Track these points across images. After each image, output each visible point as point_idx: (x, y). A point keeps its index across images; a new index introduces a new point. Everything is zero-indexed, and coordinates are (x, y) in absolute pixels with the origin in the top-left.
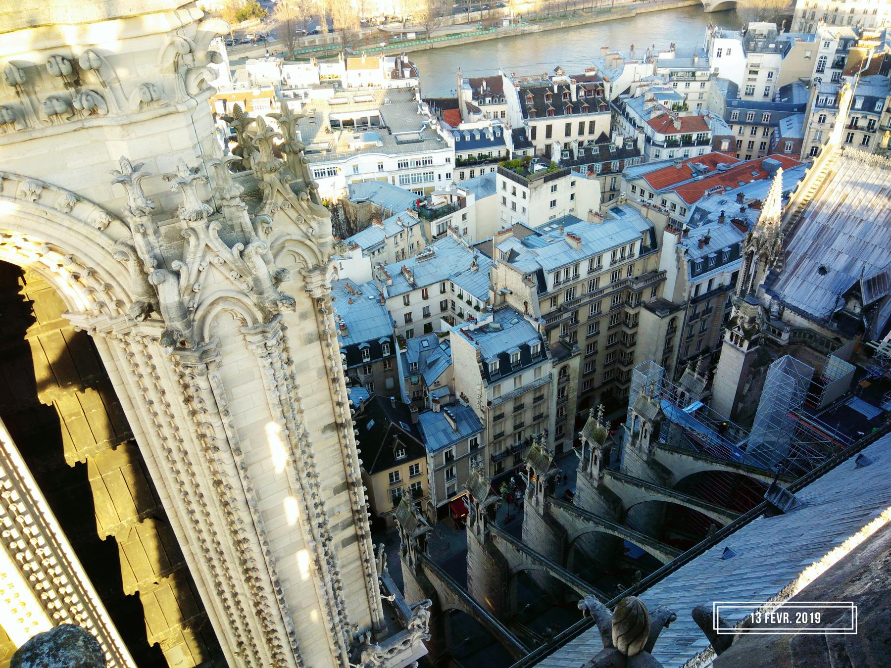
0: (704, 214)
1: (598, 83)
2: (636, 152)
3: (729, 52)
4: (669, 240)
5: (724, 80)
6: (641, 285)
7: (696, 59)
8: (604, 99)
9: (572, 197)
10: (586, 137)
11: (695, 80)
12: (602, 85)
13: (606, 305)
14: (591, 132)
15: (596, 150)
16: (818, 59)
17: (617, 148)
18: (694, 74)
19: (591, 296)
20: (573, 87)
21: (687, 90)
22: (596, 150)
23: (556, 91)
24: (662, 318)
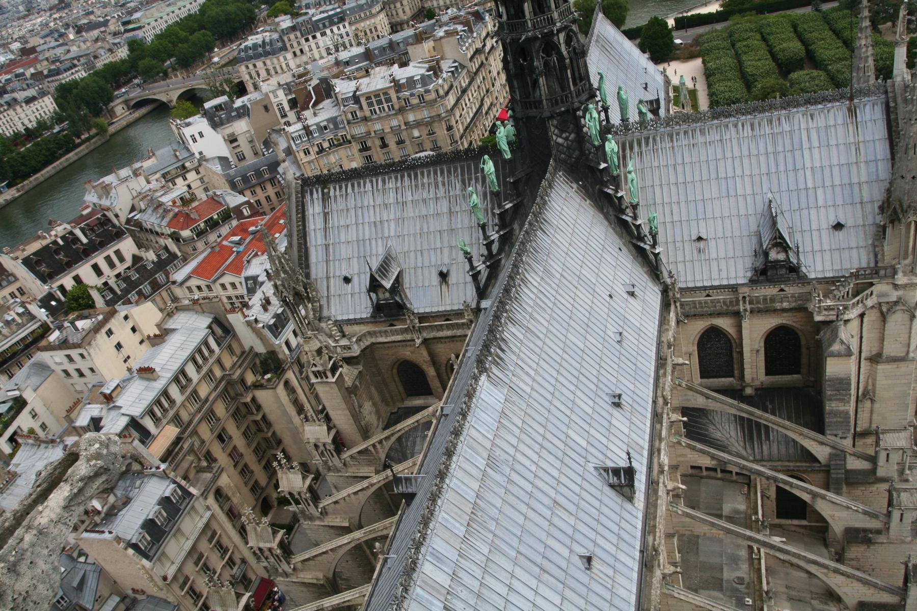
0: (254, 279)
1: (99, 216)
2: (173, 256)
3: (201, 135)
4: (236, 320)
5: (213, 159)
6: (239, 372)
7: (178, 154)
8: (114, 226)
9: (134, 330)
10: (120, 268)
11: (188, 171)
12: (104, 215)
13: (220, 409)
14: (122, 259)
15: (135, 276)
16: (276, 108)
17: (153, 262)
18: (183, 167)
19: (199, 410)
20: (78, 232)
21: (187, 182)
22: (135, 276)
23: (61, 242)
24: (275, 388)
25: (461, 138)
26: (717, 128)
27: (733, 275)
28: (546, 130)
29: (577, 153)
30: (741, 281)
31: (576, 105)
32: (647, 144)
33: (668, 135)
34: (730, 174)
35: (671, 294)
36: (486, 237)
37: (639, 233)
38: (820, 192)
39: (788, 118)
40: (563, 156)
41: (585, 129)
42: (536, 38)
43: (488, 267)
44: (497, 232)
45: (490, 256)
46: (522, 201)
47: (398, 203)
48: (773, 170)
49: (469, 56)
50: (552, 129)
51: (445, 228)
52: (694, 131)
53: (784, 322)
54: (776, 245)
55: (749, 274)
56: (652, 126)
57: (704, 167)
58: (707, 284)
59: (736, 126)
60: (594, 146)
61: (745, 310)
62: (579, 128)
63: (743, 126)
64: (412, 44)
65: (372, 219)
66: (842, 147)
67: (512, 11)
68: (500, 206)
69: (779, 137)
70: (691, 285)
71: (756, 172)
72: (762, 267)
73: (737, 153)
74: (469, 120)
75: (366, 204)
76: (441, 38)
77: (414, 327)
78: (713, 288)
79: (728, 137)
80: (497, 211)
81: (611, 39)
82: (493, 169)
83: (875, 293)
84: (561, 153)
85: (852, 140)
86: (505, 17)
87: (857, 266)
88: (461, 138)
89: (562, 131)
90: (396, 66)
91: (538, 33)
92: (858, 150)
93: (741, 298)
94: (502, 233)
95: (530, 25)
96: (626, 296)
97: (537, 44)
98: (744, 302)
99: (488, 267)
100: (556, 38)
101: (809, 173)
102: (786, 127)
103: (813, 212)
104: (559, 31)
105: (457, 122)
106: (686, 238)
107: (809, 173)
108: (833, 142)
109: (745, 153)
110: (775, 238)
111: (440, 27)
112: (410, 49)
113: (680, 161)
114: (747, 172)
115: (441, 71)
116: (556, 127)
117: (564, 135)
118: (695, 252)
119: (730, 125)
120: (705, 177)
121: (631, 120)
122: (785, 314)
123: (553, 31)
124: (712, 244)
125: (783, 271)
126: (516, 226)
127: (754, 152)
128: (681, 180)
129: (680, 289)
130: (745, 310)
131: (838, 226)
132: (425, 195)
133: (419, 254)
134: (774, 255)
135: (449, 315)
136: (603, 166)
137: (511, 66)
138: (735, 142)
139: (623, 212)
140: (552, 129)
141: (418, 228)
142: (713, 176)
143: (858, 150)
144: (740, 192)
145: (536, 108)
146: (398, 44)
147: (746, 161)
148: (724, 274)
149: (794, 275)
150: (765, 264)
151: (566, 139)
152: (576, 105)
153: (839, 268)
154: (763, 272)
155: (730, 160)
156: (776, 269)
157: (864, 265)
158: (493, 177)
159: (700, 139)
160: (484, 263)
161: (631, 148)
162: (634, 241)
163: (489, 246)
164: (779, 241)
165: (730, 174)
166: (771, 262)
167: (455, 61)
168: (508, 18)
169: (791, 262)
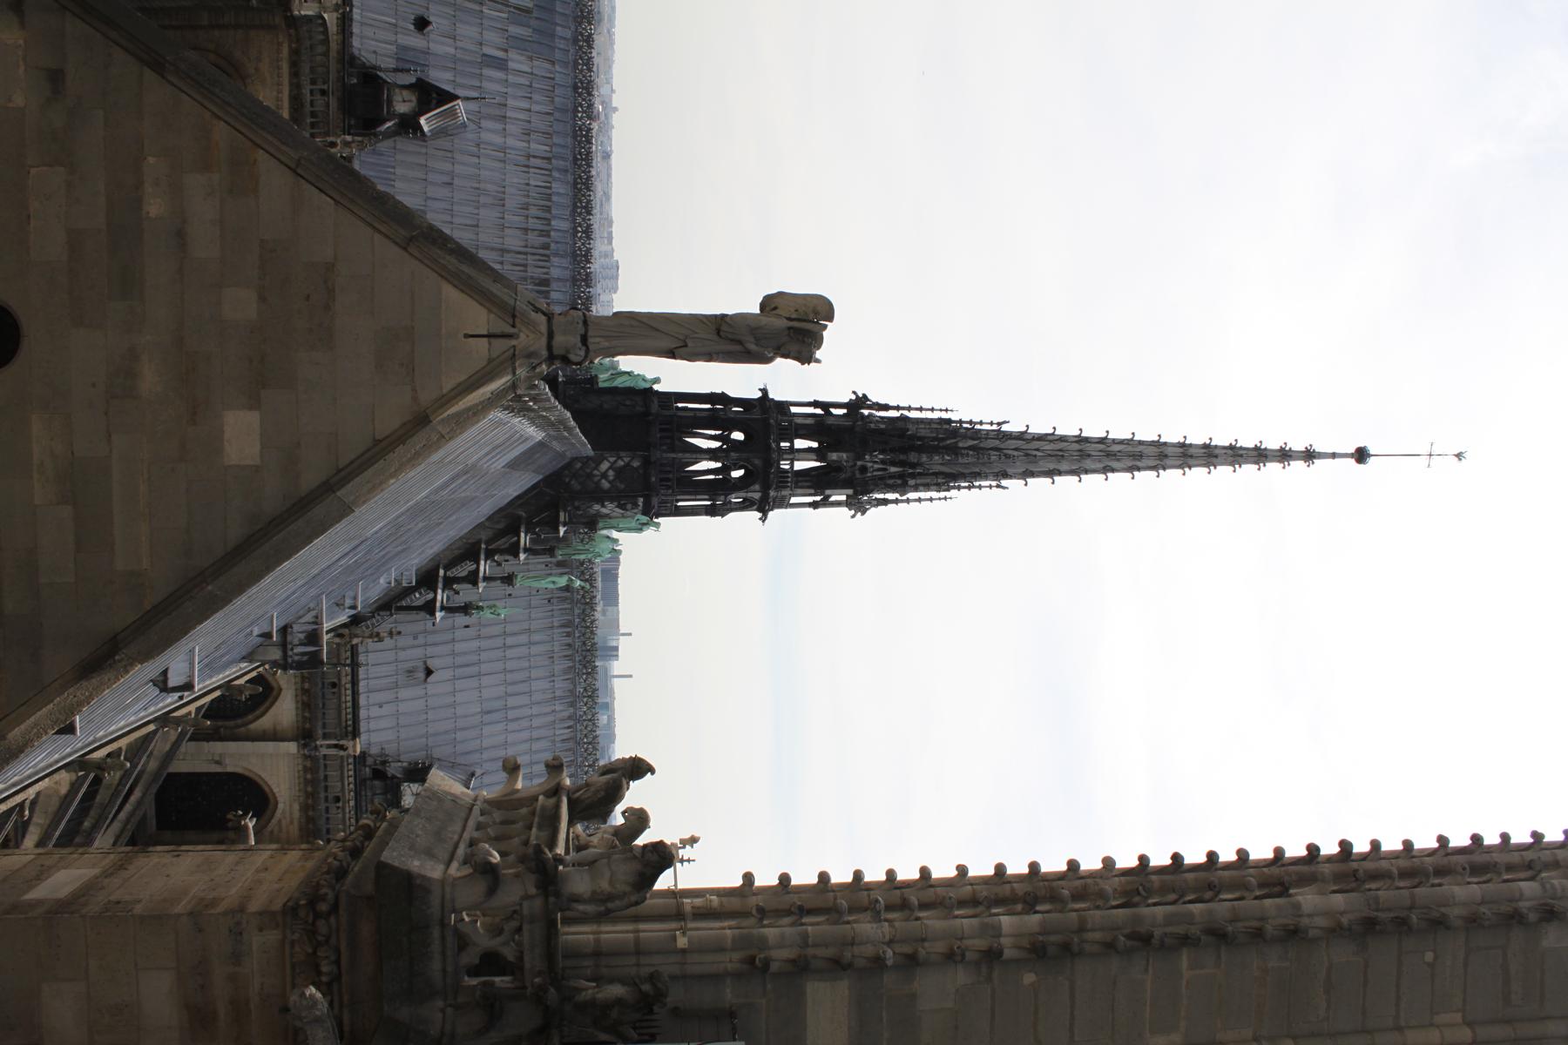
27: (373, 725)
34: (511, 714)
40: (579, 465)
47: (529, 156)
51: (482, 237)
58: (362, 684)
59: (570, 718)
65: (510, 102)
73: (536, 722)
75: (536, 97)
79: (558, 708)
89: (620, 472)
109: (535, 734)
113: (536, 637)
114: (510, 738)
116: (628, 465)
120: (510, 677)
124: (419, 691)
127: (536, 746)
133: (446, 179)
138: (551, 718)
141: (490, 187)
142: (510, 689)
144: (487, 730)
150: (394, 777)
151: (604, 476)
154: (379, 774)
155: (527, 712)
156: (385, 793)
159: (560, 665)
165: (511, 714)
166: (398, 787)
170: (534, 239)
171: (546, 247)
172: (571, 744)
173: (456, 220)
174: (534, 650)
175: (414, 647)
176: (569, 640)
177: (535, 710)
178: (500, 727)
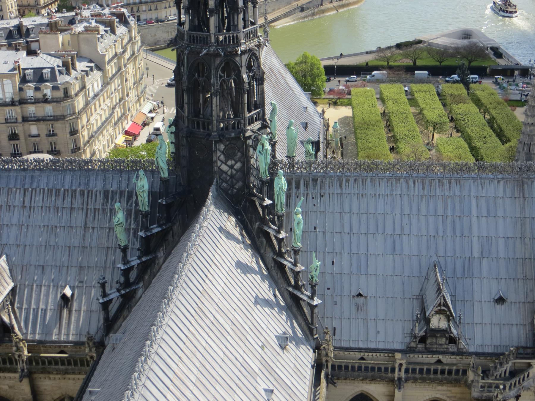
25: (85, 145)
26: (388, 181)
27: (390, 339)
28: (211, 152)
29: (240, 184)
30: (397, 346)
31: (248, 134)
32: (315, 186)
33: (339, 179)
34: (398, 231)
35: (323, 352)
36: (125, 261)
37: (296, 282)
38: (485, 262)
39: (458, 182)
40: (224, 185)
41: (252, 161)
42: (218, 55)
43: (122, 296)
44: (139, 258)
45: (127, 284)
46: (171, 228)
47: (24, 207)
48: (441, 233)
49: (107, 59)
50: (219, 153)
51: (76, 244)
52: (364, 180)
53: (438, 396)
54: (439, 312)
55: (408, 340)
56: (322, 168)
57: (372, 221)
58: (361, 345)
59: (407, 182)
60: (261, 180)
61: (400, 379)
62: (246, 159)
63: (414, 183)
64: (45, 33)
66: (508, 219)
67: (196, 22)
68: (146, 229)
69: (449, 200)
70: (344, 344)
71: (424, 232)
72: (422, 333)
73: (407, 211)
74: (95, 129)
76: (79, 33)
77: (20, 356)
78: (367, 350)
79: (399, 193)
80: (141, 234)
81: (276, 72)
82: (146, 187)
83: (531, 376)
84: (223, 181)
85: (518, 215)
86: (187, 27)
87: (515, 344)
88: (85, 145)
90: (24, 53)
91: (220, 51)
92: (523, 225)
93: (397, 366)
94: (144, 259)
95: (213, 40)
96: (278, 349)
97: (218, 61)
98: (400, 370)
99: (122, 296)
100: (237, 59)
101: (475, 240)
102: (457, 193)
103: (476, 281)
104: (243, 53)
105: (83, 127)
106: (346, 293)
107: (475, 240)
108: (500, 213)
110: (440, 305)
111: (81, 21)
112: (42, 38)
113: (347, 209)
115: (74, 68)
116: (223, 152)
117: (229, 163)
118: (354, 309)
119: (402, 180)
120: (372, 230)
121: (296, 159)
122: (440, 388)
123: (237, 51)
125: (443, 341)
126: (161, 254)
127: (424, 211)
128: (347, 230)
129: (335, 348)
130: (400, 379)
131: (501, 300)
132: (59, 203)
134: (438, 322)
135: (65, 347)
136: (268, 202)
137: (185, 78)
139: (281, 254)
140: (219, 153)
142: (380, 231)
143: (523, 225)
144: (406, 252)
145: (204, 128)
146: (28, 29)
147: (414, 220)
148: (381, 337)
149: (452, 348)
150: (425, 332)
151: (231, 167)
152: (248, 134)
153: (498, 344)
154: (423, 340)
155: (398, 216)
157: (523, 344)
158: (146, 195)
160: (118, 291)
161: (298, 187)
162: (290, 289)
163: (126, 273)
164: (443, 308)
165: (398, 231)
166: (432, 330)
167: (91, 61)
168: (190, 30)
169: (452, 333)
170: (78, 202)
171: (82, 193)
172: (427, 182)
173: (66, 265)
174: (355, 209)
175: (341, 305)
176: (352, 180)
177: (398, 211)
178: (405, 238)
